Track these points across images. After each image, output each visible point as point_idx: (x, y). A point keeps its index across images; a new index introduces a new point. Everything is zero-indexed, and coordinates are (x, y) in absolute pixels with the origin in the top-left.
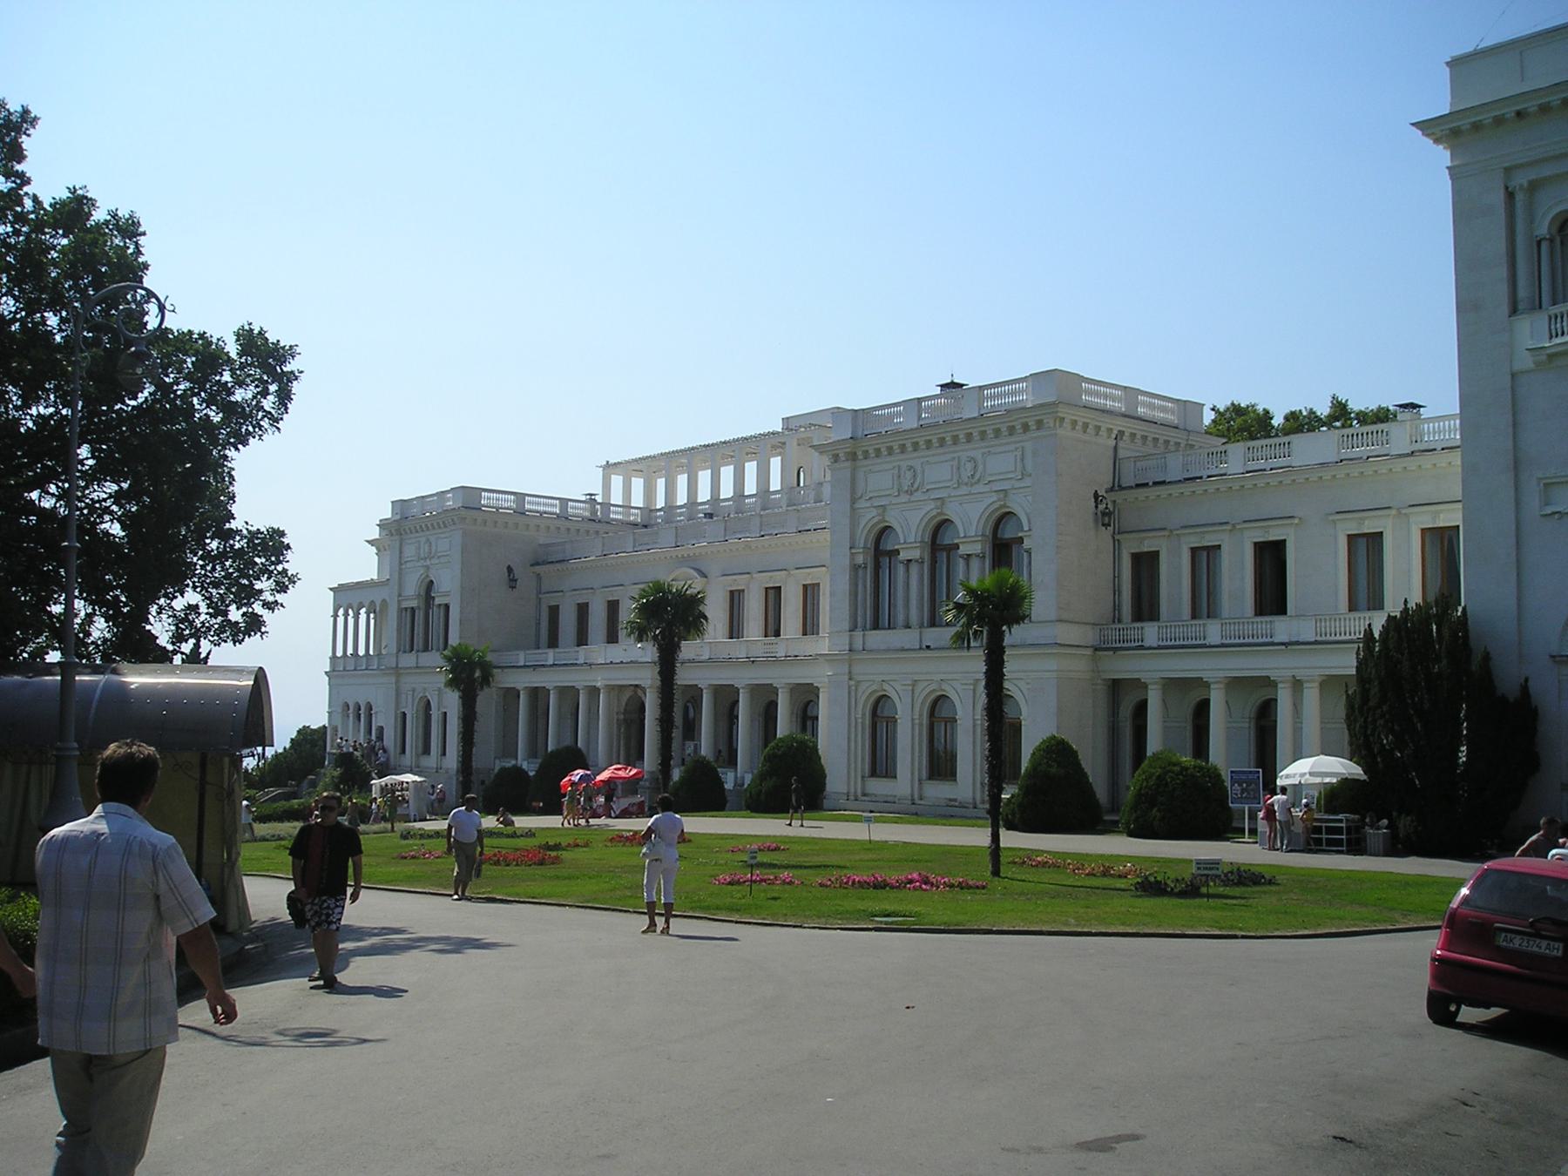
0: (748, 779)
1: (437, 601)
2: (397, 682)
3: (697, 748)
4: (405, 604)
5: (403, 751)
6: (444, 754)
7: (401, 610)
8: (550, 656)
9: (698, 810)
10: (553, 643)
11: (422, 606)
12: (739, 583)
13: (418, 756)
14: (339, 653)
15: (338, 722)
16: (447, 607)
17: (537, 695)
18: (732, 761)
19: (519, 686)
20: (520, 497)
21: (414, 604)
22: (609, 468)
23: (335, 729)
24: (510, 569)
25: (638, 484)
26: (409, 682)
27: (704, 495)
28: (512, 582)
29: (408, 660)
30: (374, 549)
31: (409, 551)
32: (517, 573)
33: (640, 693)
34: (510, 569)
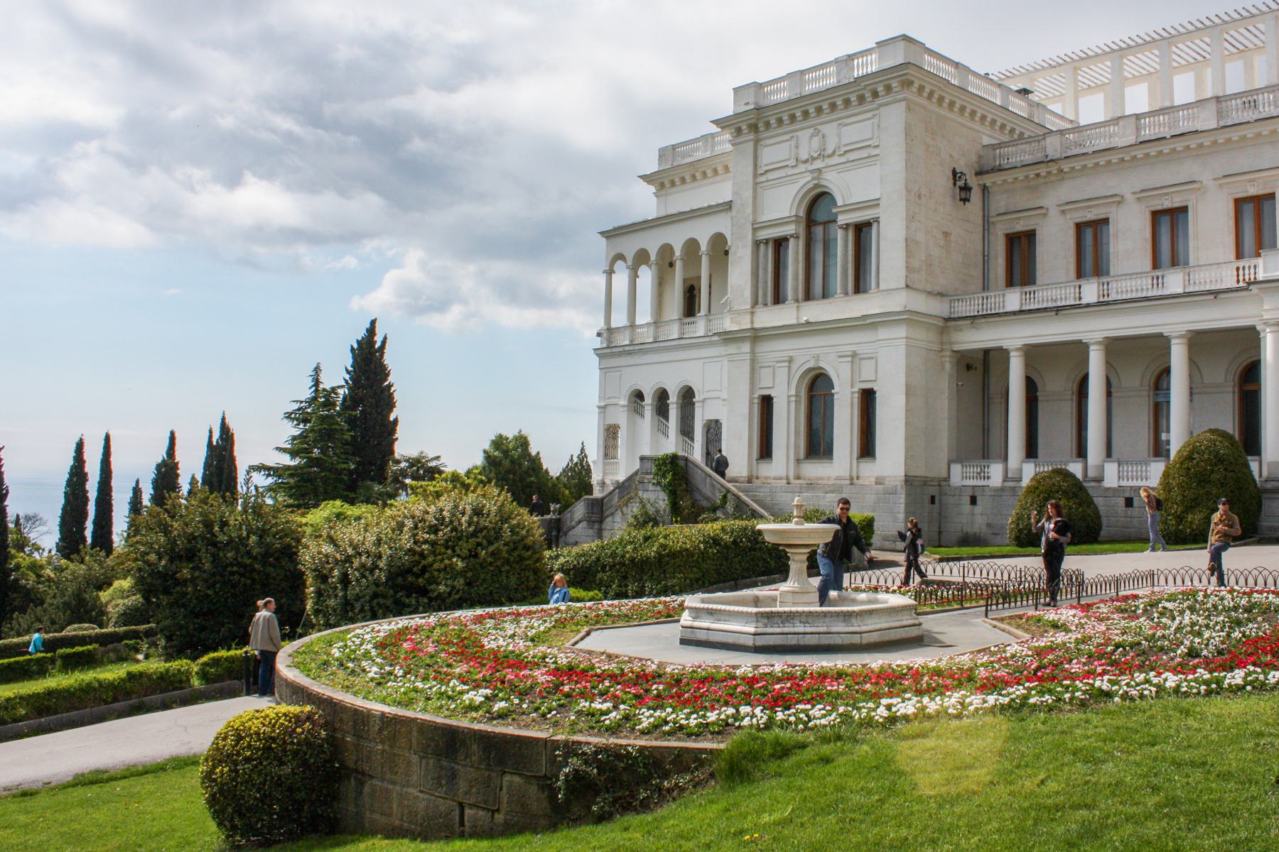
1: (842, 219)
2: (753, 352)
4: (764, 234)
7: (757, 244)
13: (798, 461)
14: (619, 319)
15: (621, 418)
21: (789, 229)
26: (773, 350)
29: (772, 317)
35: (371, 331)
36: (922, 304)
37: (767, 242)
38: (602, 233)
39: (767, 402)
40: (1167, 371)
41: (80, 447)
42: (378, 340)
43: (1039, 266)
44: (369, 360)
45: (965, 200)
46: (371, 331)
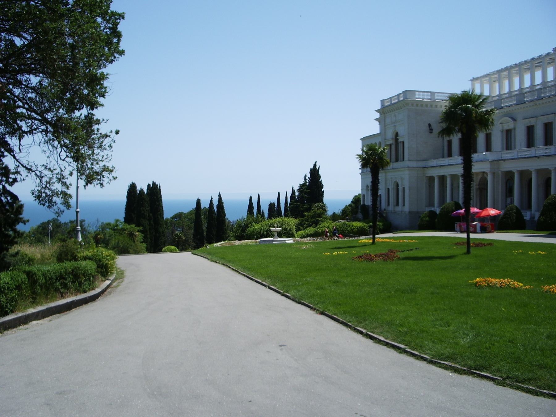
0: (537, 215)
1: (400, 140)
2: (385, 176)
3: (512, 202)
5: (389, 205)
6: (404, 205)
8: (447, 161)
9: (506, 230)
10: (450, 155)
11: (394, 144)
12: (532, 122)
13: (394, 206)
16: (403, 142)
17: (442, 179)
18: (529, 207)
19: (434, 175)
20: (432, 93)
21: (390, 142)
22: (474, 79)
23: (364, 196)
24: (430, 125)
25: (486, 87)
27: (516, 87)
28: (431, 130)
30: (378, 123)
31: (388, 121)
32: (433, 126)
33: (485, 175)
34: (430, 125)
35: (315, 165)
36: (414, 164)
37: (388, 145)
38: (361, 139)
39: (389, 189)
40: (531, 179)
41: (251, 198)
42: (317, 167)
43: (478, 146)
44: (315, 172)
45: (431, 133)
46: (315, 165)
